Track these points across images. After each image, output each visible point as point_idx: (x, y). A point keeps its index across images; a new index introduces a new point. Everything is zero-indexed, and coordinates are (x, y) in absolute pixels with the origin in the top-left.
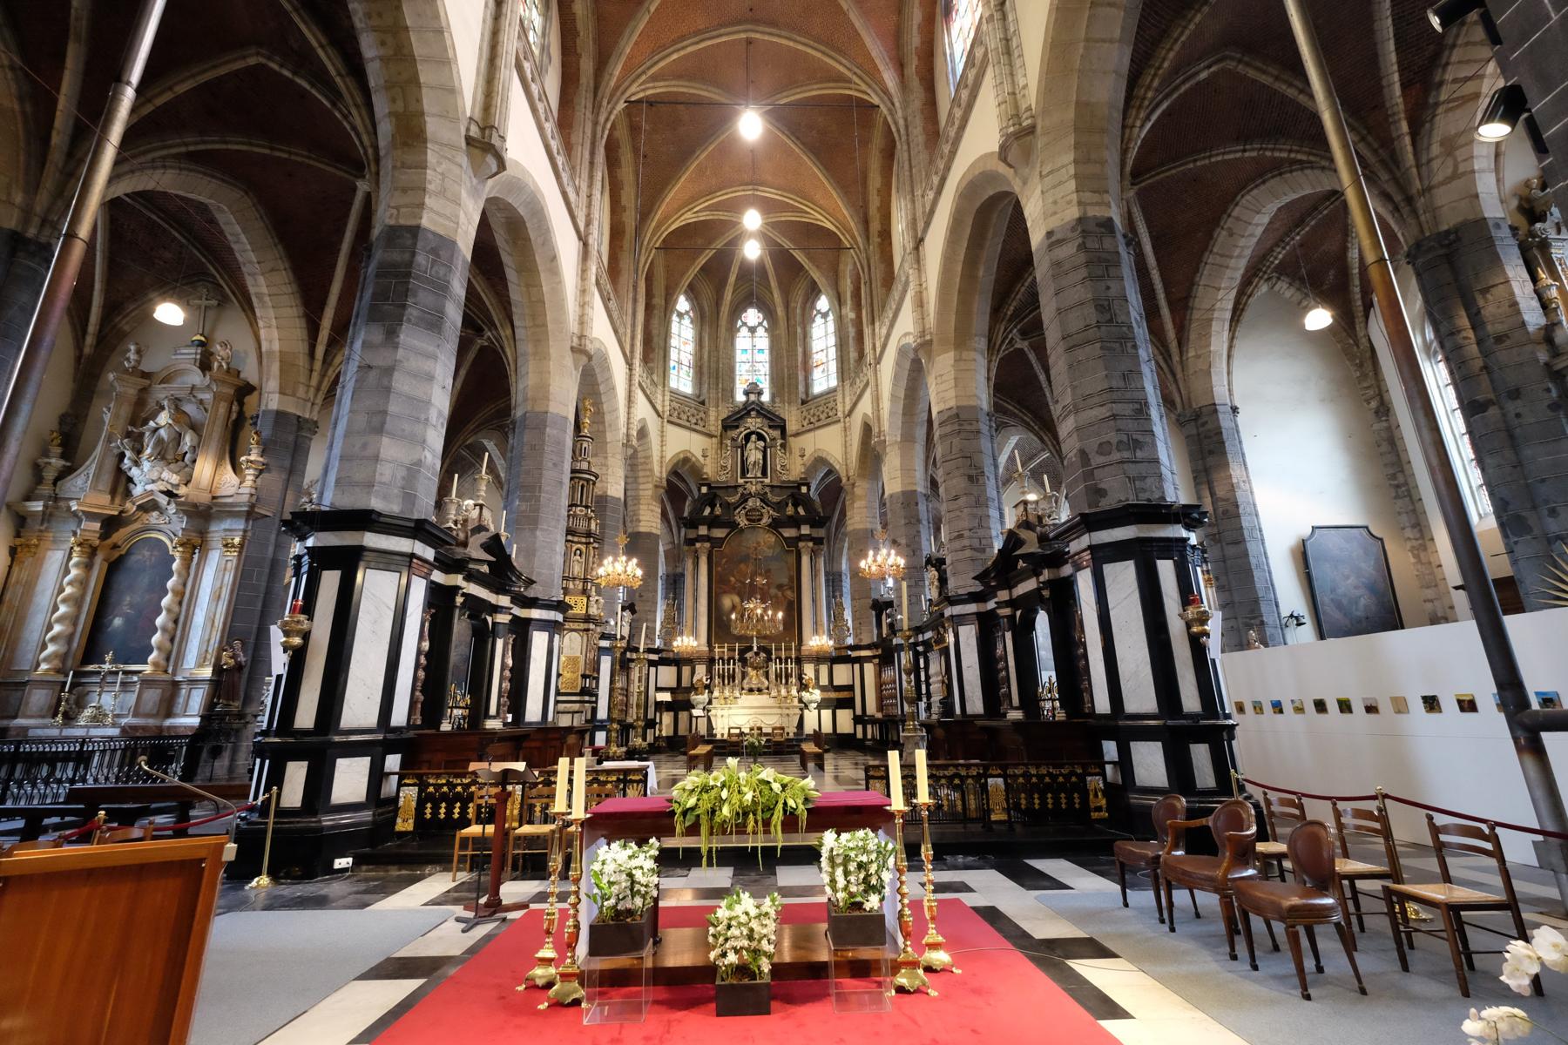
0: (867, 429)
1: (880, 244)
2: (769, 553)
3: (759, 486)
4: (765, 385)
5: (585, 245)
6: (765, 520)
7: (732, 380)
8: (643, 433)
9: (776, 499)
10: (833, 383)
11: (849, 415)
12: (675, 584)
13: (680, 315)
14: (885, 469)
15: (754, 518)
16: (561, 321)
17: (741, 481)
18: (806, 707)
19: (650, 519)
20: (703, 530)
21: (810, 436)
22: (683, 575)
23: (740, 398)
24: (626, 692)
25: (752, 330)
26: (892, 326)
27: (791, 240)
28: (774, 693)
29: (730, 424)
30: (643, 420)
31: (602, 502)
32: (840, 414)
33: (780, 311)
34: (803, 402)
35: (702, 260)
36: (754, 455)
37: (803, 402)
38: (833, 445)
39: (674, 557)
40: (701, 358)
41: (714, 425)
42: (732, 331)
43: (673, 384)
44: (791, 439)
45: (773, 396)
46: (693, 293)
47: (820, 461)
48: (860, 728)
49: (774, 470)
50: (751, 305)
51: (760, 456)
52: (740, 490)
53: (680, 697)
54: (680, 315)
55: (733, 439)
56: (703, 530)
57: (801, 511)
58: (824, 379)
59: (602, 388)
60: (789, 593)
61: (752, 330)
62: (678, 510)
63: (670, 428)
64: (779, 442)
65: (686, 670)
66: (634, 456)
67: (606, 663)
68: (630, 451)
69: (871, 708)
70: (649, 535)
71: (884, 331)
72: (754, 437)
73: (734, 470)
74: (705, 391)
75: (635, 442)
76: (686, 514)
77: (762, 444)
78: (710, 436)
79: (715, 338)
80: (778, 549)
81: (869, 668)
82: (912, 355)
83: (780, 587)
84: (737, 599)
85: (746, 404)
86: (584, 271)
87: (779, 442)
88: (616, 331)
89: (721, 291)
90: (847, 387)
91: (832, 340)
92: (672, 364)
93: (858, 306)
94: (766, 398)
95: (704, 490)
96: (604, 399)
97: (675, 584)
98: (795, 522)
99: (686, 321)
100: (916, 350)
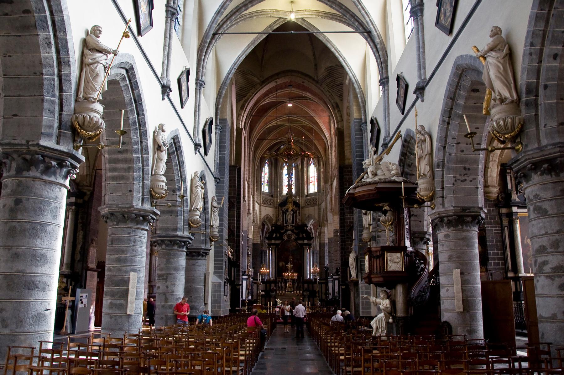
9: (297, 231)
17: (285, 225)
20: (273, 242)
49: (296, 221)
65: (268, 285)
79: (276, 173)
84: (284, 263)
98: (303, 239)
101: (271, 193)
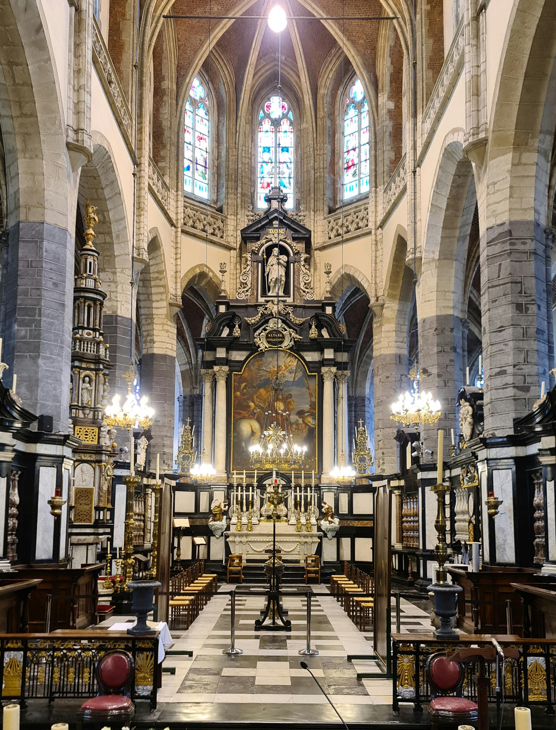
0: (401, 244)
1: (429, 14)
2: (290, 378)
3: (281, 306)
4: (289, 191)
5: (78, 10)
6: (287, 343)
7: (253, 184)
8: (154, 245)
9: (299, 321)
10: (365, 188)
11: (381, 226)
12: (192, 407)
13: (194, 103)
14: (419, 290)
15: (275, 339)
16: (52, 109)
17: (261, 300)
18: (325, 535)
19: (165, 340)
21: (338, 248)
22: (200, 397)
23: (262, 205)
24: (143, 517)
25: (276, 123)
26: (438, 119)
27: (324, 8)
28: (293, 521)
29: (250, 235)
30: (155, 229)
31: (112, 322)
32: (371, 225)
33: (308, 100)
34: (331, 211)
35: (218, 33)
36: (276, 271)
37: (331, 211)
38: (365, 262)
39: (192, 378)
40: (219, 157)
41: (233, 237)
42: (253, 125)
43: (188, 188)
44: (317, 253)
45: (298, 203)
46: (209, 72)
47: (348, 278)
50: (274, 90)
51: (282, 272)
52: (261, 310)
53: (198, 523)
54: (194, 103)
55: (253, 253)
56: (221, 353)
57: (325, 334)
59: (107, 193)
61: (276, 123)
62: (195, 330)
63: (185, 240)
64: (304, 256)
65: (204, 496)
66: (145, 271)
67: (121, 491)
68: (139, 267)
70: (164, 357)
71: (428, 126)
72: (276, 251)
74: (223, 196)
75: (145, 256)
76: (203, 335)
77: (284, 258)
78: (229, 248)
80: (300, 374)
82: (460, 156)
83: (301, 413)
84: (256, 425)
85: (268, 213)
86: (77, 46)
87: (304, 256)
88: (120, 124)
89: (238, 74)
91: (366, 137)
92: (186, 163)
93: (396, 94)
94: (289, 205)
95: (222, 309)
96: (110, 205)
97: (192, 407)
98: (318, 345)
99: (201, 112)
100: (467, 151)
101: (216, 202)
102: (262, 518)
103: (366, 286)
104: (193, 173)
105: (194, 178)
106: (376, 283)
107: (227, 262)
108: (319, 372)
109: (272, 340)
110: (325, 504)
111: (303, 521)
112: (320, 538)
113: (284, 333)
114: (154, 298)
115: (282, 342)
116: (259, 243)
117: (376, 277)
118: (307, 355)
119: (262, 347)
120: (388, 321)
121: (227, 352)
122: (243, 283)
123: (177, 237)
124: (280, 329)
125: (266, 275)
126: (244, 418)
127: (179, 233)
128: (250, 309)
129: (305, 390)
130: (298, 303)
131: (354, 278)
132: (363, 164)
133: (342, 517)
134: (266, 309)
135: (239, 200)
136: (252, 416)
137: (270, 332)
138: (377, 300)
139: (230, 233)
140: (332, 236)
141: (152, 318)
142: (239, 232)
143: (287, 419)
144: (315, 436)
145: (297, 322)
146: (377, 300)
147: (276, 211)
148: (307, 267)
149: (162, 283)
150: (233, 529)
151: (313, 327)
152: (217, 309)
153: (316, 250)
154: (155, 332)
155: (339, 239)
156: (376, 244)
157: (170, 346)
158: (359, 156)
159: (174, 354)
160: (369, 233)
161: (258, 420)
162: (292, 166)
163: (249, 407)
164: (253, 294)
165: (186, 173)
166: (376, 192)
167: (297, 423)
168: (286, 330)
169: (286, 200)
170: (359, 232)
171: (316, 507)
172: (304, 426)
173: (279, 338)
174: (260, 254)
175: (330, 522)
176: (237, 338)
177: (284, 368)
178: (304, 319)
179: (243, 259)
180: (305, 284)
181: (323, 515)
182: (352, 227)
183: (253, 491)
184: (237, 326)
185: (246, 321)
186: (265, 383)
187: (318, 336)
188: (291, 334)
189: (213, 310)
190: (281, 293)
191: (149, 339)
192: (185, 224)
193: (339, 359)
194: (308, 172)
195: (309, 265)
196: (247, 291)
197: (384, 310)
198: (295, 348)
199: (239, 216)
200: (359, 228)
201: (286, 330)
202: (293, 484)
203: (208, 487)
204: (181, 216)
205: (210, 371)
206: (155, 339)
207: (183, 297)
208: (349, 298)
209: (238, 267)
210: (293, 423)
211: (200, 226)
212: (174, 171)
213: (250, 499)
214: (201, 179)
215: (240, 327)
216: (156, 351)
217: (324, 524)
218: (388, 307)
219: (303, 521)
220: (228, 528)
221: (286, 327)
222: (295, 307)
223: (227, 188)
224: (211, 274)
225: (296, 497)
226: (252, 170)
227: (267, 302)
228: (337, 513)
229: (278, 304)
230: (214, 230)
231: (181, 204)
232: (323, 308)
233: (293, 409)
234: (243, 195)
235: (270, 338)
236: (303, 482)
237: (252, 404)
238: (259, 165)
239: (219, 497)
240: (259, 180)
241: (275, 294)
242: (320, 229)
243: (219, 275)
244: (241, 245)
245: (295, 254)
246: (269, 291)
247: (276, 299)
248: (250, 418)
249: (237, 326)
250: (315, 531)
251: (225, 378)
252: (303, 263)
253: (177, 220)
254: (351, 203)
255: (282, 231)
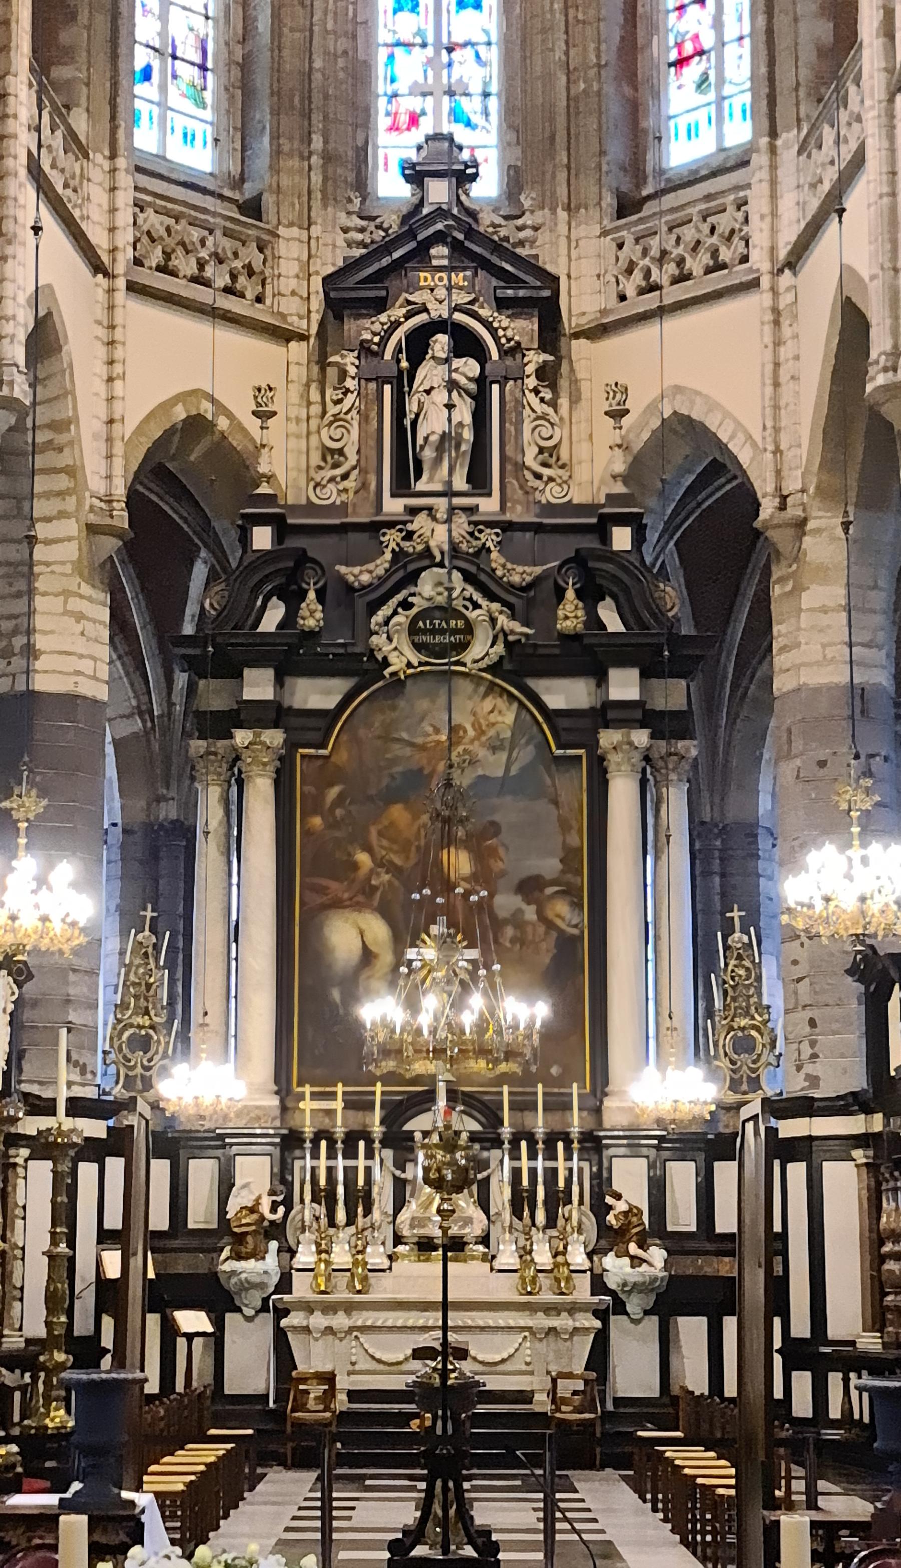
2: (494, 765)
3: (461, 523)
4: (484, 144)
6: (481, 650)
7: (363, 118)
9: (520, 574)
10: (740, 132)
15: (440, 635)
17: (394, 506)
18: (619, 1307)
23: (391, 187)
28: (507, 1257)
29: (352, 293)
32: (759, 260)
34: (626, 207)
37: (626, 207)
38: (739, 376)
40: (247, 33)
41: (297, 296)
43: (145, 139)
44: (580, 347)
45: (514, 181)
48: (803, 1381)
49: (513, 466)
51: (464, 413)
52: (392, 538)
53: (182, 1265)
55: (365, 349)
56: (258, 686)
57: (612, 622)
58: (701, 117)
60: (561, 909)
63: (138, 314)
64: (535, 359)
69: (846, 1317)
72: (441, 343)
73: (368, 466)
74: (261, 161)
77: (469, 367)
80: (525, 755)
81: (843, 1181)
83: (530, 887)
84: (378, 929)
85: (413, 216)
87: (535, 359)
90: (788, 154)
92: (141, 57)
94: (487, 187)
95: (263, 538)
98: (588, 656)
101: (239, 182)
102: (401, 1248)
103: (744, 457)
104: (163, 88)
105: (163, 105)
106: (777, 451)
107: (278, 383)
108: (592, 745)
109: (428, 639)
110: (618, 1197)
111: (543, 1257)
112: (602, 1314)
113: (472, 615)
114: (40, 508)
115: (463, 647)
116: (383, 318)
117: (777, 430)
118: (548, 691)
119: (397, 664)
120: (823, 573)
121: (279, 682)
122: (332, 452)
123: (111, 308)
124: (458, 604)
125: (408, 422)
126: (337, 904)
127: (121, 296)
128: (353, 537)
129: (542, 806)
130: (517, 514)
131: (706, 429)
132: (731, 51)
133: (677, 1244)
134: (409, 536)
135: (317, 178)
136: (364, 896)
137: (423, 615)
138: (783, 507)
139: (288, 284)
140: (630, 292)
141: (30, 577)
142: (317, 283)
143: (484, 906)
144: (577, 970)
145: (516, 579)
146: (783, 507)
147: (440, 213)
148: (547, 394)
149: (64, 459)
150: (302, 1288)
151: (570, 594)
152: (245, 539)
153: (576, 335)
154: (39, 622)
155: (651, 301)
156: (777, 323)
157: (86, 666)
158: (718, 24)
159: (102, 693)
160: (754, 284)
161: (385, 912)
162: (493, 55)
163: (355, 866)
164: (364, 486)
165: (140, 89)
166: (773, 150)
167: (516, 920)
168: (476, 606)
169: (474, 177)
170: (718, 280)
171: (586, 1208)
172: (541, 929)
173: (455, 632)
174: (388, 355)
175: (636, 1261)
176: (312, 635)
177: (471, 733)
178: (538, 570)
179: (332, 372)
180: (541, 450)
181: (610, 1238)
182: (696, 264)
183: (370, 1155)
184: (312, 595)
185: (342, 579)
186: (410, 786)
187: (585, 623)
188: (493, 621)
189: (229, 540)
190: (460, 483)
191: (19, 642)
192: (138, 262)
193: (659, 704)
194: (548, 78)
195: (553, 387)
196: (345, 477)
197: (807, 540)
198: (507, 666)
199: (316, 230)
200: (720, 266)
201: (476, 606)
202: (506, 1131)
203: (216, 1142)
204: (125, 237)
205: (221, 744)
206: (40, 642)
207: (133, 500)
208: (691, 491)
209: (315, 396)
210: (506, 921)
211: (186, 265)
212: (102, 89)
213: (361, 1182)
214: (188, 106)
215: (321, 597)
216: (41, 684)
217: (616, 1268)
218: (818, 531)
219: (543, 1257)
220: (285, 1284)
221: (477, 597)
222: (507, 527)
223: (275, 137)
224: (223, 423)
225: (516, 1173)
226: (360, 74)
227: (414, 511)
228: (657, 1230)
229: (448, 521)
230: (234, 277)
231: (125, 198)
232: (602, 528)
233: (503, 874)
234: (328, 158)
235: (425, 632)
236: (539, 1124)
237: (363, 858)
238: (382, 54)
239: (254, 1176)
240: (382, 103)
241: (438, 487)
242: (586, 268)
243: (253, 425)
244: (322, 324)
245: (504, 353)
246: (418, 476)
247: (442, 504)
248: (358, 907)
249: (312, 595)
250: (582, 1291)
251: (271, 769)
252: (531, 382)
253: (113, 250)
254: (692, 179)
255: (458, 278)
